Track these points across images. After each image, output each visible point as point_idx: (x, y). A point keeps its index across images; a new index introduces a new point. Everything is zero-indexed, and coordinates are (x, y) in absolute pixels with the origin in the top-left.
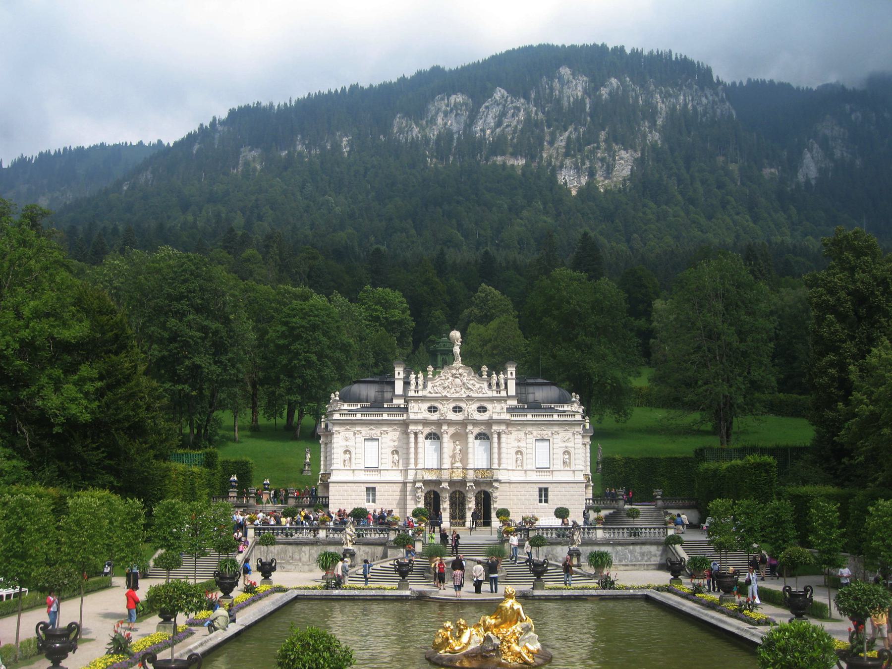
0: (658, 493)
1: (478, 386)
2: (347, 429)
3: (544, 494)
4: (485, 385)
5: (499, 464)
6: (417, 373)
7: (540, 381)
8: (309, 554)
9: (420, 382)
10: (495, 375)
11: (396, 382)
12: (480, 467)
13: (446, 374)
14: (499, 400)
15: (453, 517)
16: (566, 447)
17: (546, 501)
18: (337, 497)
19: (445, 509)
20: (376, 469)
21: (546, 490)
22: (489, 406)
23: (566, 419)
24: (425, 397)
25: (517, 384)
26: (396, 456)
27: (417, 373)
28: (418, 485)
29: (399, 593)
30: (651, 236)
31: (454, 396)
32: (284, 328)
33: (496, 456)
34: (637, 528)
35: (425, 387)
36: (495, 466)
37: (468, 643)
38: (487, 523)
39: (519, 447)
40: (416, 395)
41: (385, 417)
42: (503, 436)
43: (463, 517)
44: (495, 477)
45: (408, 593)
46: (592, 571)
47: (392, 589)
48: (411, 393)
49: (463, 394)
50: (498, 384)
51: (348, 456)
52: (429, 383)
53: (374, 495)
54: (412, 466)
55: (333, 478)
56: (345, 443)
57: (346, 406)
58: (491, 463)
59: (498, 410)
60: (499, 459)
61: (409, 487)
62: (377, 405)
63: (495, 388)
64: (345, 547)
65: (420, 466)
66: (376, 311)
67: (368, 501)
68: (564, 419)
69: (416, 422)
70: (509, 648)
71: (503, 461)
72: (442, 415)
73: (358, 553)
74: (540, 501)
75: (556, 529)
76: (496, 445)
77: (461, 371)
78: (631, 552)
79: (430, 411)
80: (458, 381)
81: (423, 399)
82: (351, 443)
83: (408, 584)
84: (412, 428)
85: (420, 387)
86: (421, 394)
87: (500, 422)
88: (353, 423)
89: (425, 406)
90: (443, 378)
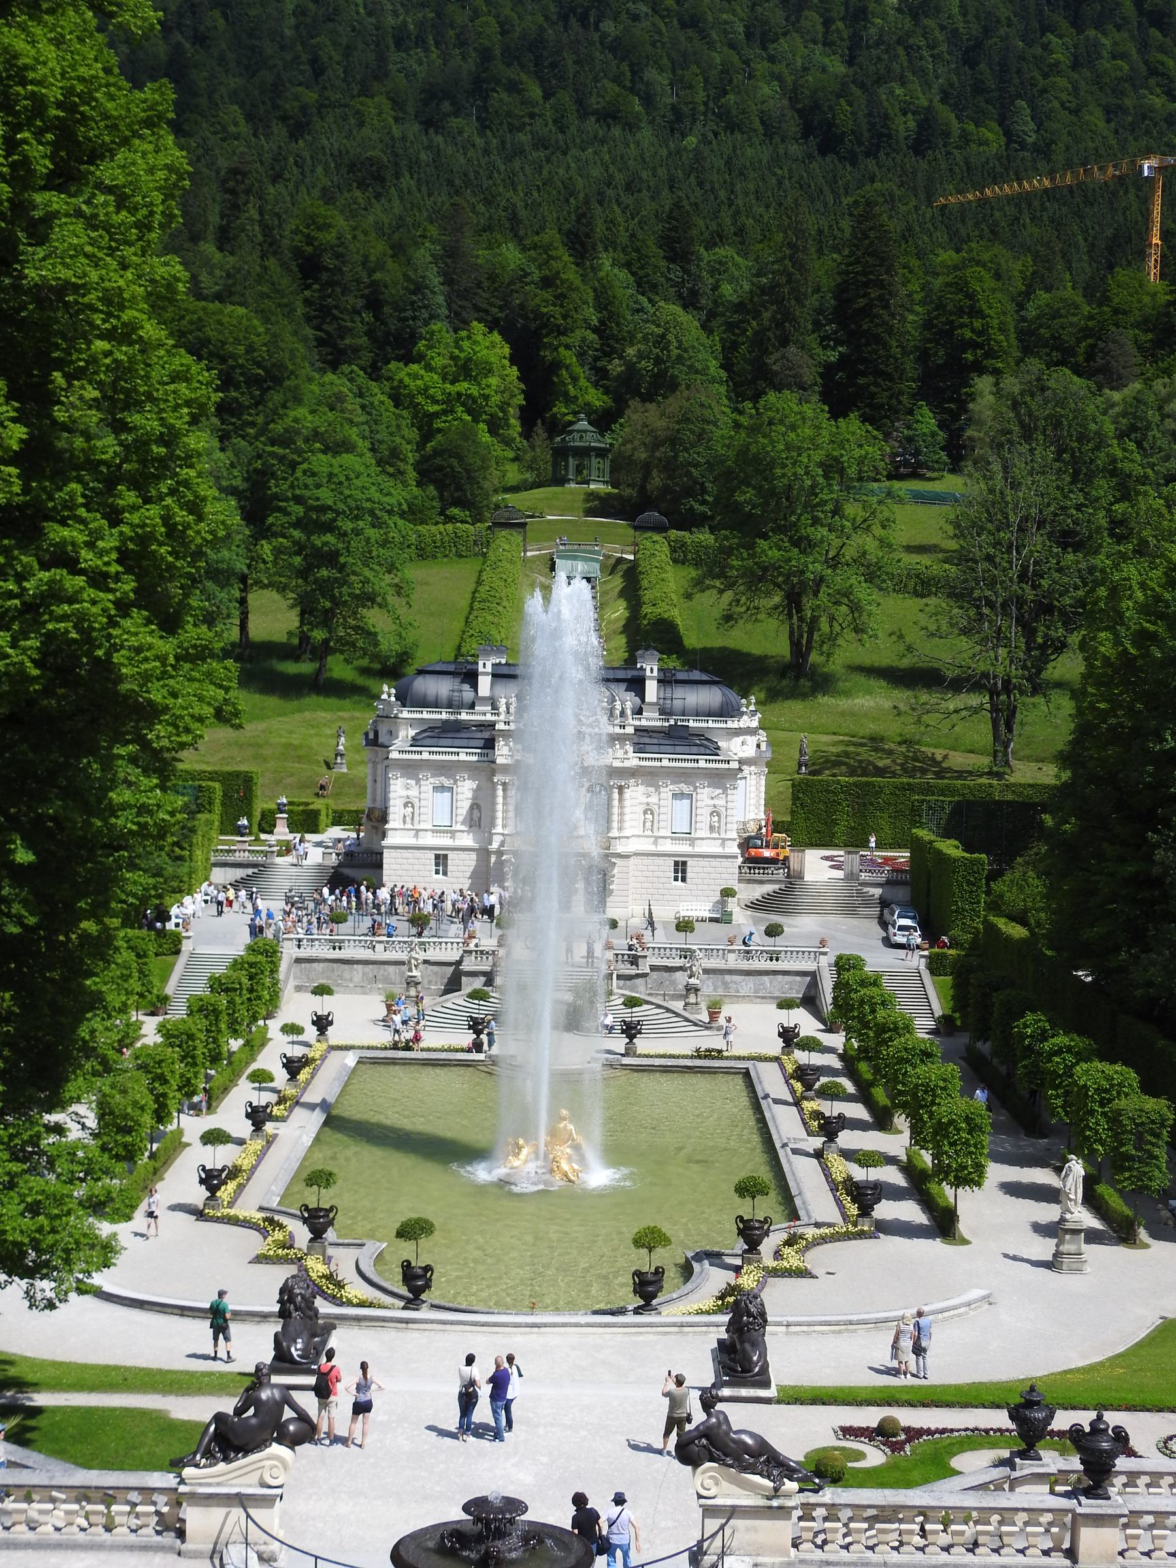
5: (620, 829)
7: (696, 675)
17: (684, 880)
21: (684, 863)
25: (659, 681)
30: (1056, 104)
50: (623, 714)
55: (389, 840)
56: (405, 793)
57: (405, 714)
60: (621, 821)
74: (676, 879)
82: (414, 792)
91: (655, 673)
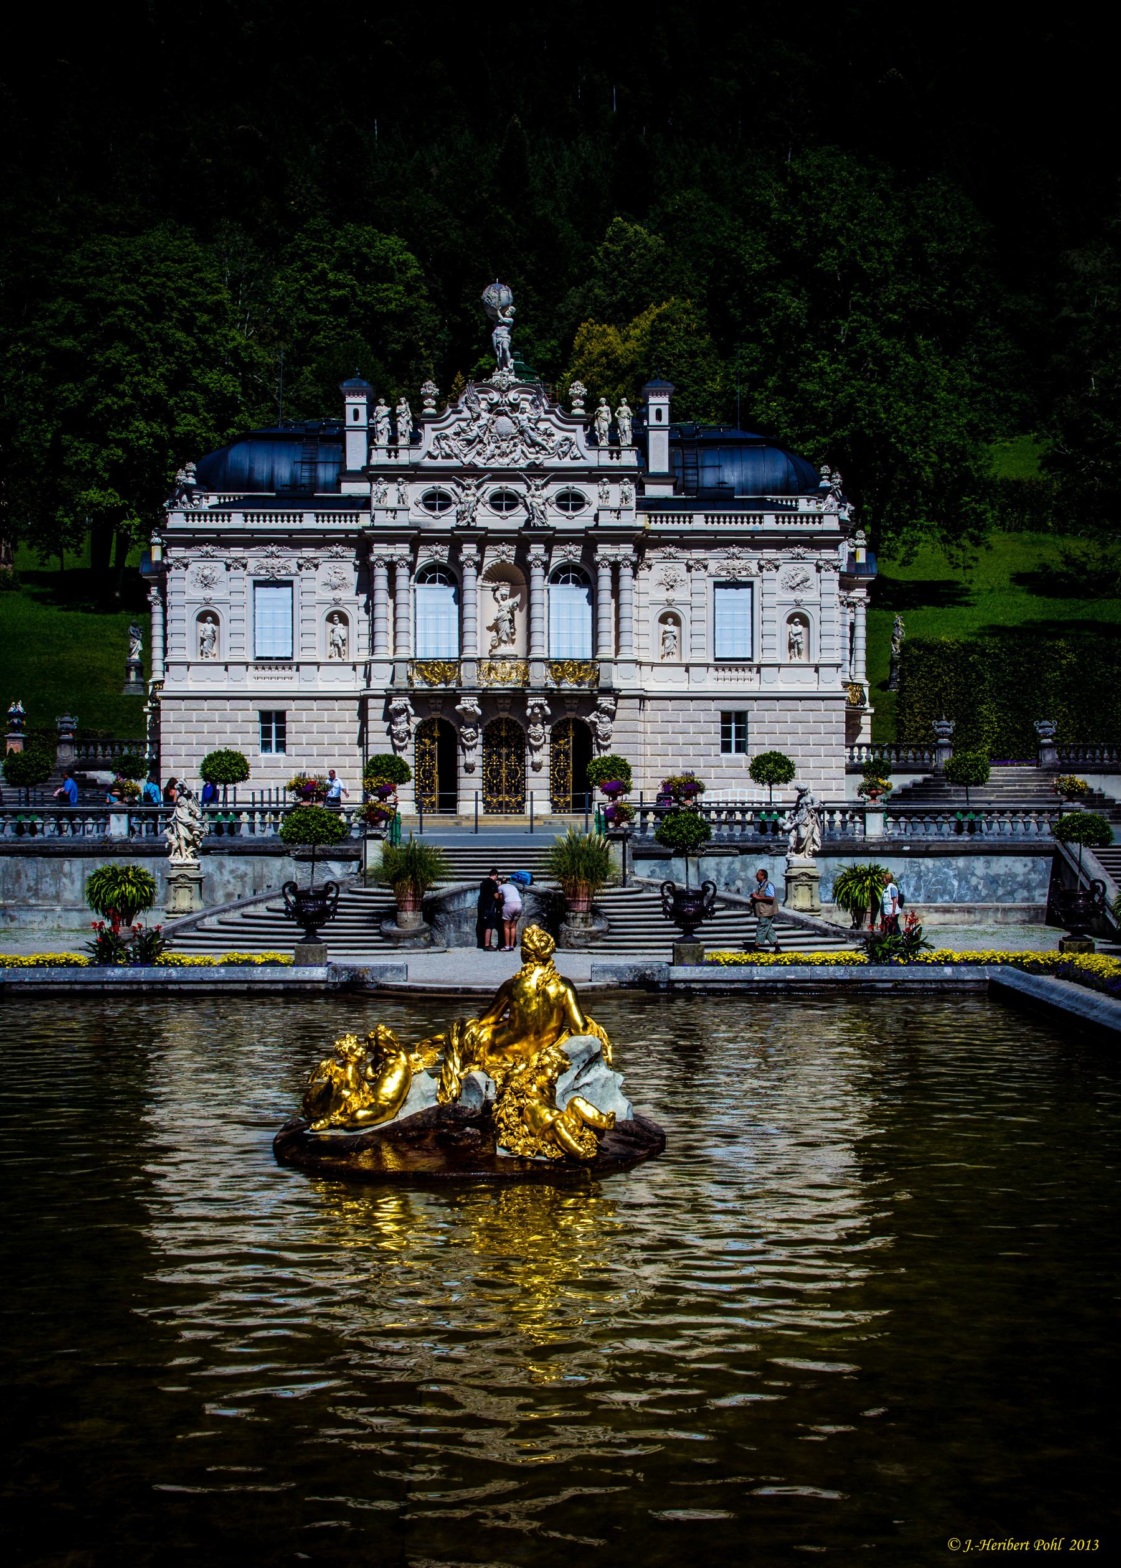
0: (1047, 728)
1: (559, 436)
2: (207, 555)
3: (734, 727)
4: (579, 435)
6: (392, 404)
8: (76, 875)
9: (404, 425)
10: (605, 409)
11: (349, 435)
12: (564, 655)
13: (476, 404)
14: (615, 476)
15: (491, 786)
16: (798, 604)
18: (183, 738)
19: (469, 768)
20: (285, 663)
21: (741, 717)
22: (590, 491)
23: (798, 527)
24: (415, 466)
25: (672, 443)
26: (340, 628)
27: (392, 404)
28: (397, 703)
29: (293, 973)
31: (495, 464)
32: (69, 306)
33: (607, 625)
34: (977, 812)
35: (415, 439)
36: (607, 652)
37: (401, 1098)
38: (581, 804)
39: (669, 603)
40: (392, 461)
41: (309, 521)
42: (626, 572)
43: (518, 787)
44: (603, 683)
45: (319, 973)
46: (844, 919)
47: (273, 963)
48: (380, 458)
49: (520, 457)
51: (209, 627)
52: (428, 427)
53: (281, 732)
54: (385, 652)
56: (201, 594)
58: (595, 647)
59: (614, 502)
61: (376, 709)
62: (297, 496)
63: (604, 442)
64: (175, 859)
65: (403, 653)
66: (338, 285)
67: (266, 746)
68: (792, 527)
69: (392, 537)
70: (520, 1111)
71: (625, 639)
72: (460, 515)
73: (217, 877)
74: (726, 747)
75: (757, 812)
76: (605, 596)
77: (512, 395)
78: (962, 876)
79: (431, 507)
80: (504, 424)
81: (414, 473)
82: (216, 594)
83: (323, 952)
84: (380, 550)
85: (403, 441)
86: (404, 458)
87: (617, 536)
88: (223, 540)
89: (416, 491)
90: (466, 414)
91: (665, 420)
